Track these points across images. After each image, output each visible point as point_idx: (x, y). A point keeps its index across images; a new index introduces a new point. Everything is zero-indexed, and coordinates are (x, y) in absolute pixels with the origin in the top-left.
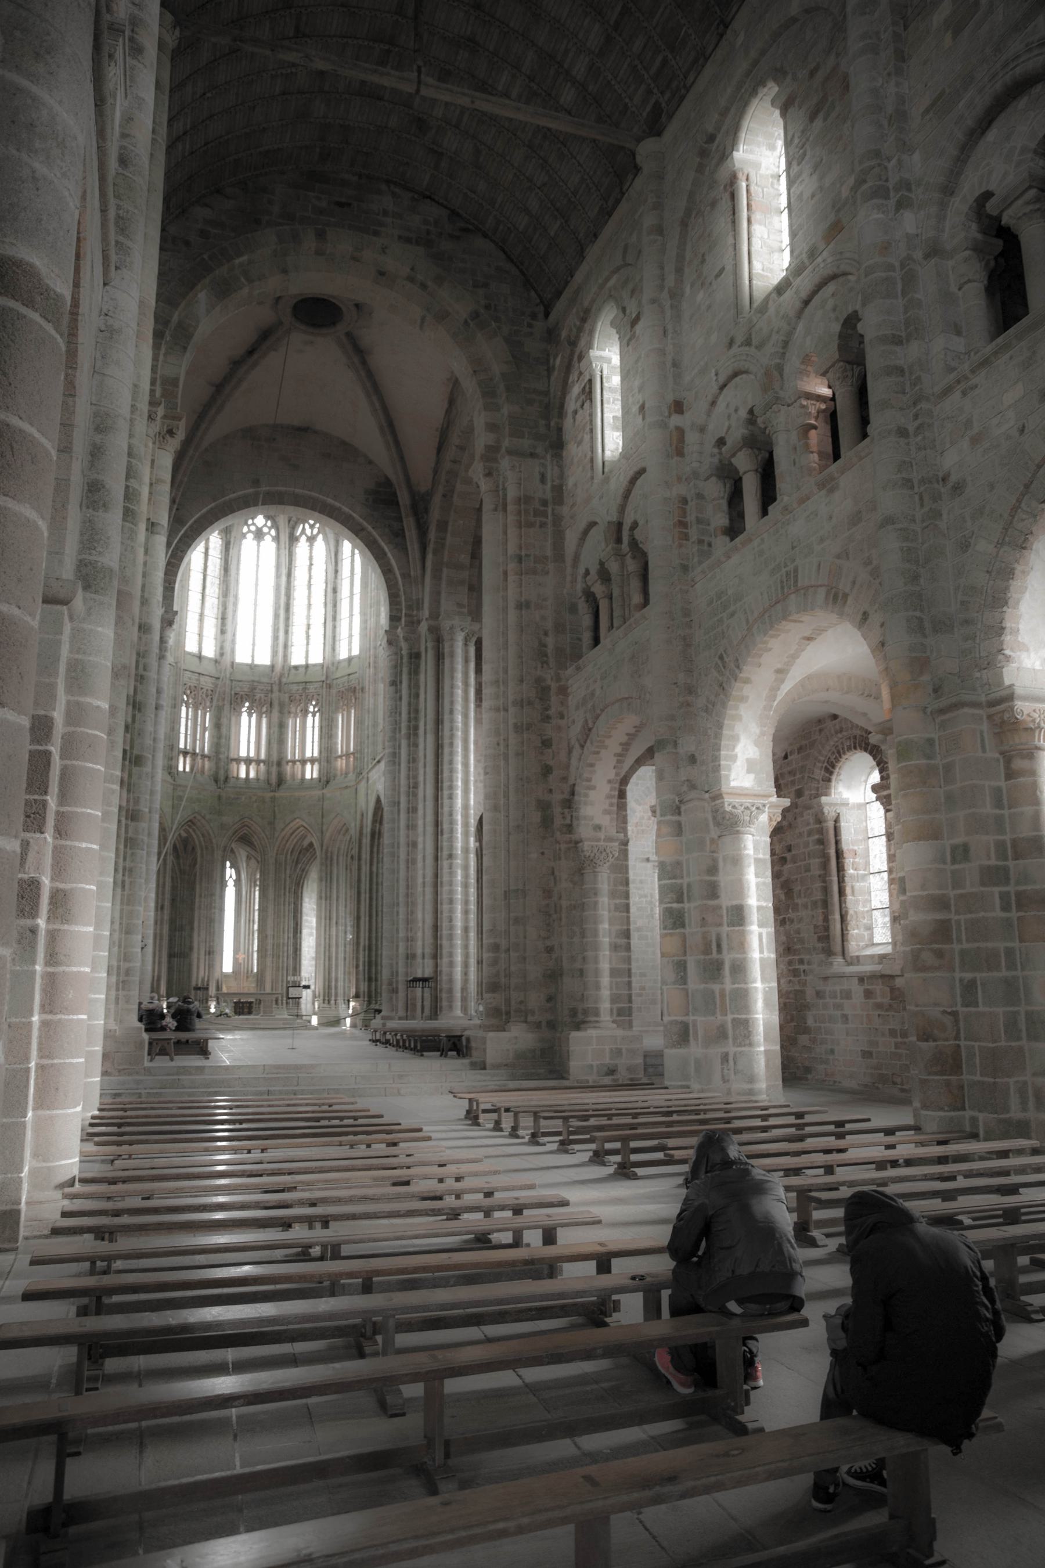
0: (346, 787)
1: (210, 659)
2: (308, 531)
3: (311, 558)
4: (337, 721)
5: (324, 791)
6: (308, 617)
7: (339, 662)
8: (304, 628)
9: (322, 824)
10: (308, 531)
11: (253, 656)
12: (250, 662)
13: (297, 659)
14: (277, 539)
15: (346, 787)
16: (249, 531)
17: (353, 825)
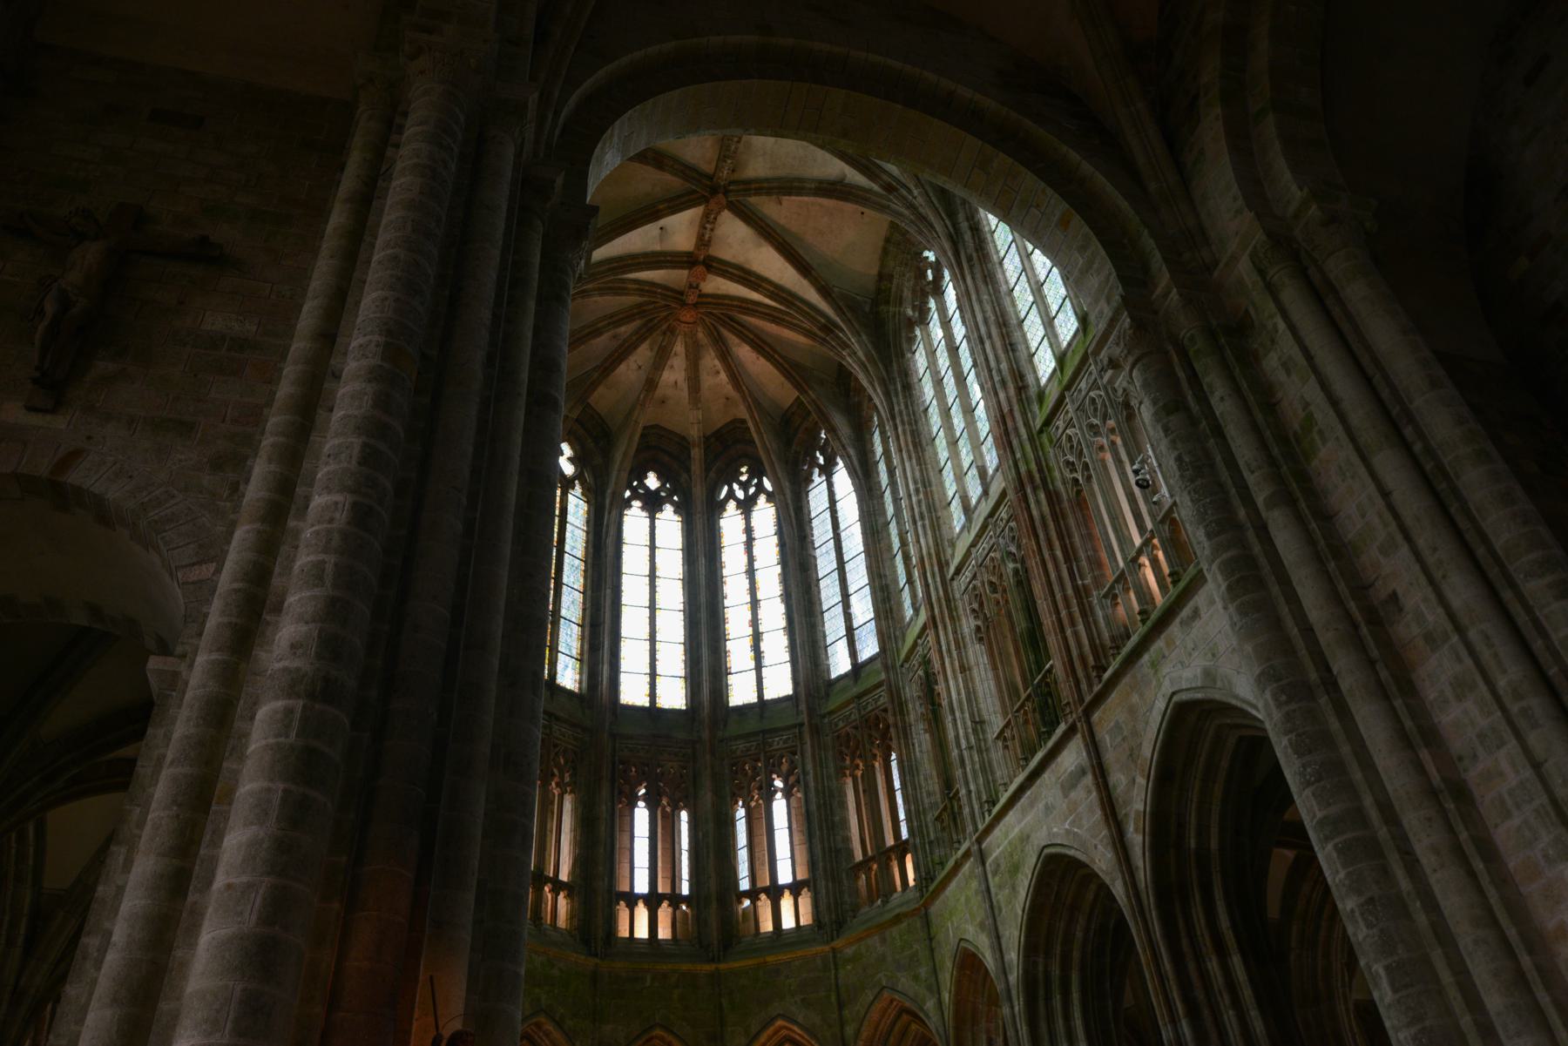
0: (898, 919)
1: (570, 693)
2: (740, 494)
3: (749, 530)
4: (843, 794)
5: (837, 943)
6: (755, 622)
7: (832, 684)
8: (748, 642)
9: (842, 1023)
10: (740, 494)
11: (653, 695)
12: (645, 702)
13: (741, 692)
14: (681, 509)
15: (898, 919)
16: (635, 496)
17: (930, 1005)
